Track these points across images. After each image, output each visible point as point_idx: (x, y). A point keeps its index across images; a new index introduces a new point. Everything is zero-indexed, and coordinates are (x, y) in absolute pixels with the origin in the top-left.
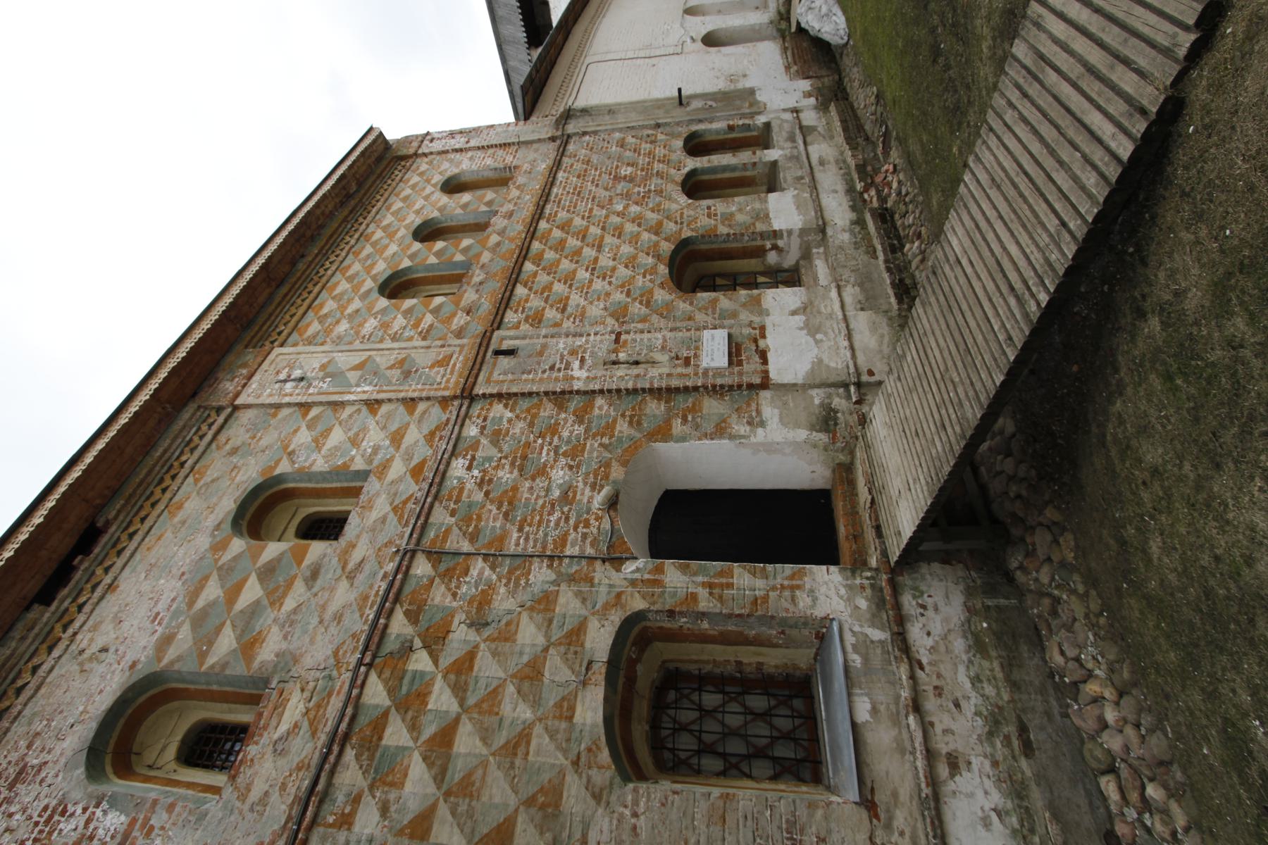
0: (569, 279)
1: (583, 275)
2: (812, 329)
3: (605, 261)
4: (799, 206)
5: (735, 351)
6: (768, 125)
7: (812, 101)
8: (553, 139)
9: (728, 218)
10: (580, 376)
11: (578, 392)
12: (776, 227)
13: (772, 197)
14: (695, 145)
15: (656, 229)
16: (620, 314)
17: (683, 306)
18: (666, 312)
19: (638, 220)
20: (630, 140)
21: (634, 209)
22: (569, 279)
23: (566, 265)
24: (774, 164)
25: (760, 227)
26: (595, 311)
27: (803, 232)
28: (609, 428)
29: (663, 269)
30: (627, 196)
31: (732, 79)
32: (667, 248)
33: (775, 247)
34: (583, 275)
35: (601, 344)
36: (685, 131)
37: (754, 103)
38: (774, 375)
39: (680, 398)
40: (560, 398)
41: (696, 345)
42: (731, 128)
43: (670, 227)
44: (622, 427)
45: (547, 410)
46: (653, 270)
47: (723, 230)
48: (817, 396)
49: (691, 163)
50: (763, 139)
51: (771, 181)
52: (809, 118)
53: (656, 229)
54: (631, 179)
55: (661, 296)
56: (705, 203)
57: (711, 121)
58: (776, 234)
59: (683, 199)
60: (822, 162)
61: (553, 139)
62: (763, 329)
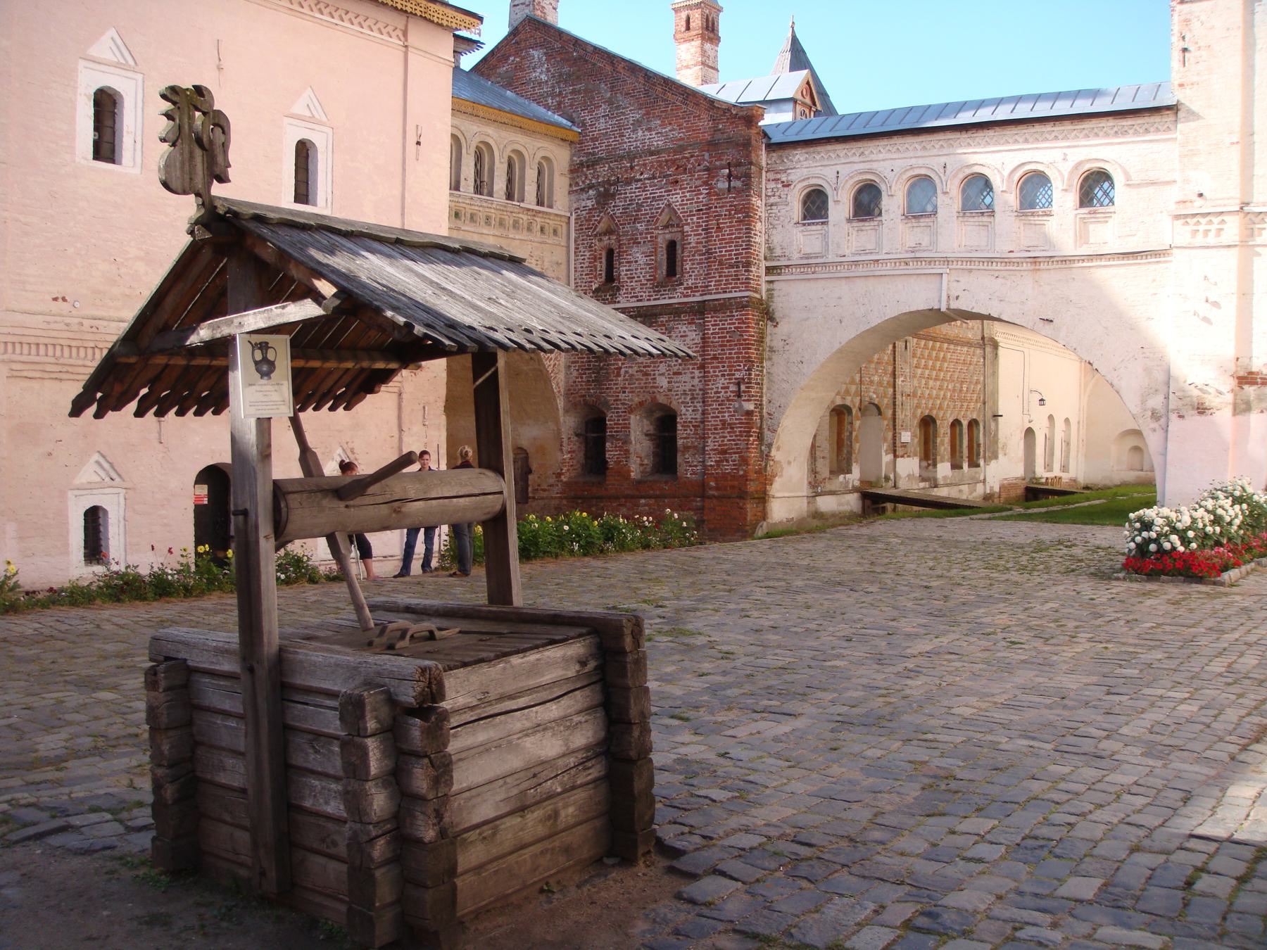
0: (926, 367)
1: (927, 372)
2: (909, 476)
3: (931, 383)
4: (945, 478)
5: (904, 445)
6: (978, 466)
7: (988, 491)
8: (983, 338)
9: (942, 442)
10: (899, 381)
11: (895, 381)
12: (939, 466)
13: (948, 465)
14: (973, 424)
15: (940, 408)
16: (915, 395)
17: (916, 422)
18: (914, 415)
19: (944, 398)
20: (979, 386)
21: (949, 394)
22: (926, 367)
23: (930, 363)
24: (961, 468)
25: (938, 458)
26: (916, 382)
27: (935, 479)
28: (885, 397)
29: (927, 413)
30: (954, 390)
31: (1005, 446)
32: (934, 413)
33: (929, 465)
34: (927, 372)
35: (908, 390)
36: (980, 420)
37: (991, 459)
38: (899, 460)
39: (891, 423)
40: (894, 375)
41: (906, 430)
42: (979, 445)
43: (941, 414)
44: (886, 401)
45: (890, 369)
46: (927, 408)
47: (939, 440)
48: (892, 476)
49: (965, 423)
50: (974, 464)
51: (956, 466)
52: (980, 488)
53: (940, 408)
54: (961, 391)
55: (919, 411)
56: (949, 431)
57: (984, 435)
58: (935, 465)
59: (951, 420)
60: (960, 491)
61: (983, 338)
62: (909, 456)
